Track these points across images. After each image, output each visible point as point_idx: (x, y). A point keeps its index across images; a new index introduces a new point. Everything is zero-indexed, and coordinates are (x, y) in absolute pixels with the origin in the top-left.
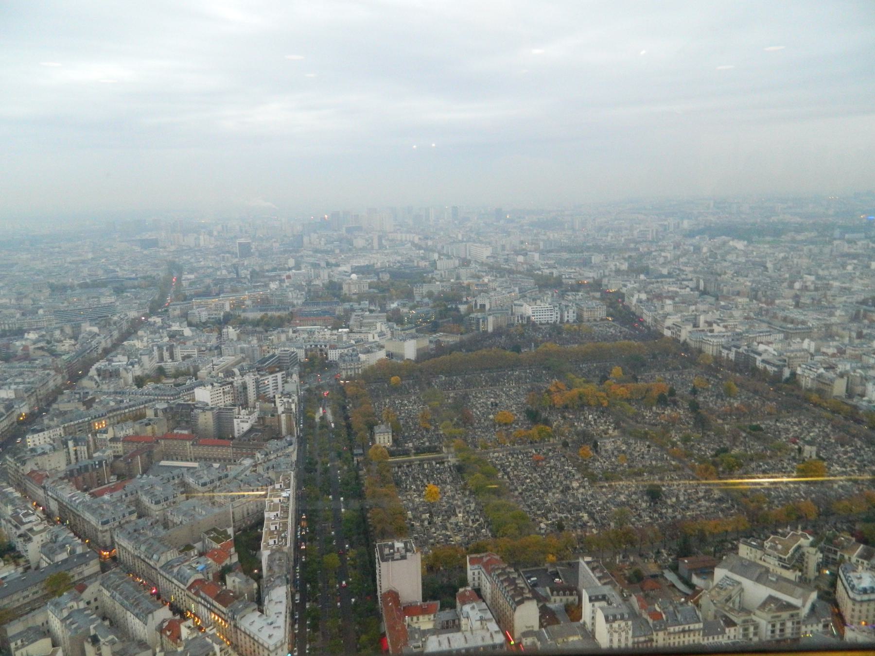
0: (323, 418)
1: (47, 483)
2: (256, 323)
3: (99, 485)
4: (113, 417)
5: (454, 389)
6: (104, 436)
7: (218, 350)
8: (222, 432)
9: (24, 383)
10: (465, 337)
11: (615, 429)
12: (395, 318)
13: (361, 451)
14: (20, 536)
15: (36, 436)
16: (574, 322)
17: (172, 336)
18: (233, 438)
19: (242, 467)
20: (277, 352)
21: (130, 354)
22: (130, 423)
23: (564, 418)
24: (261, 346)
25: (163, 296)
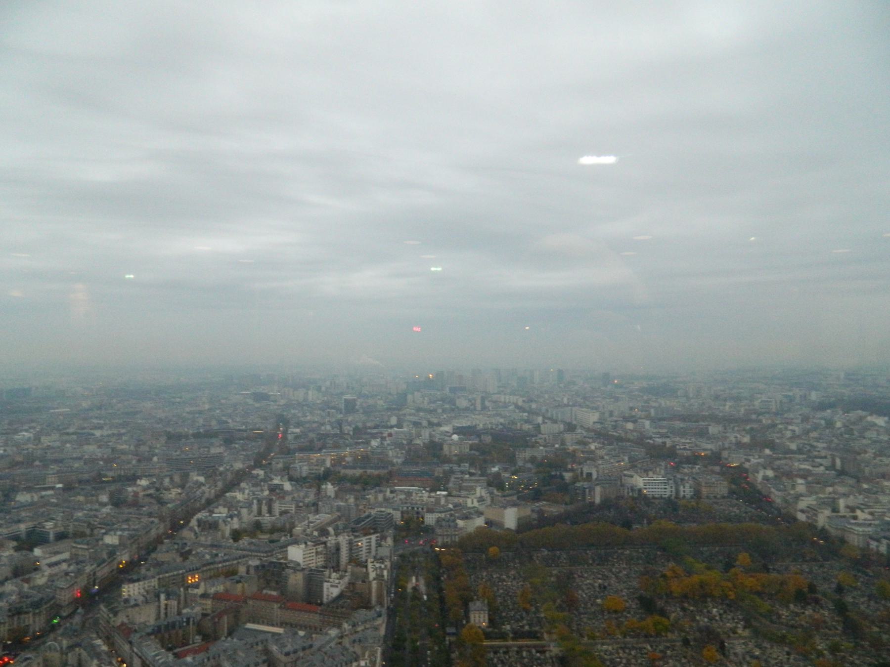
0: (415, 589)
1: (135, 638)
2: (355, 481)
3: (184, 645)
4: (206, 571)
5: (558, 566)
6: (196, 591)
7: (315, 507)
8: (311, 595)
9: (128, 530)
10: (570, 508)
11: (745, 628)
12: (496, 483)
13: (453, 630)
15: (131, 585)
16: (692, 498)
17: (273, 489)
18: (321, 604)
19: (328, 638)
20: (373, 512)
21: (231, 505)
22: (222, 579)
23: (684, 609)
24: (357, 505)
25: (269, 449)
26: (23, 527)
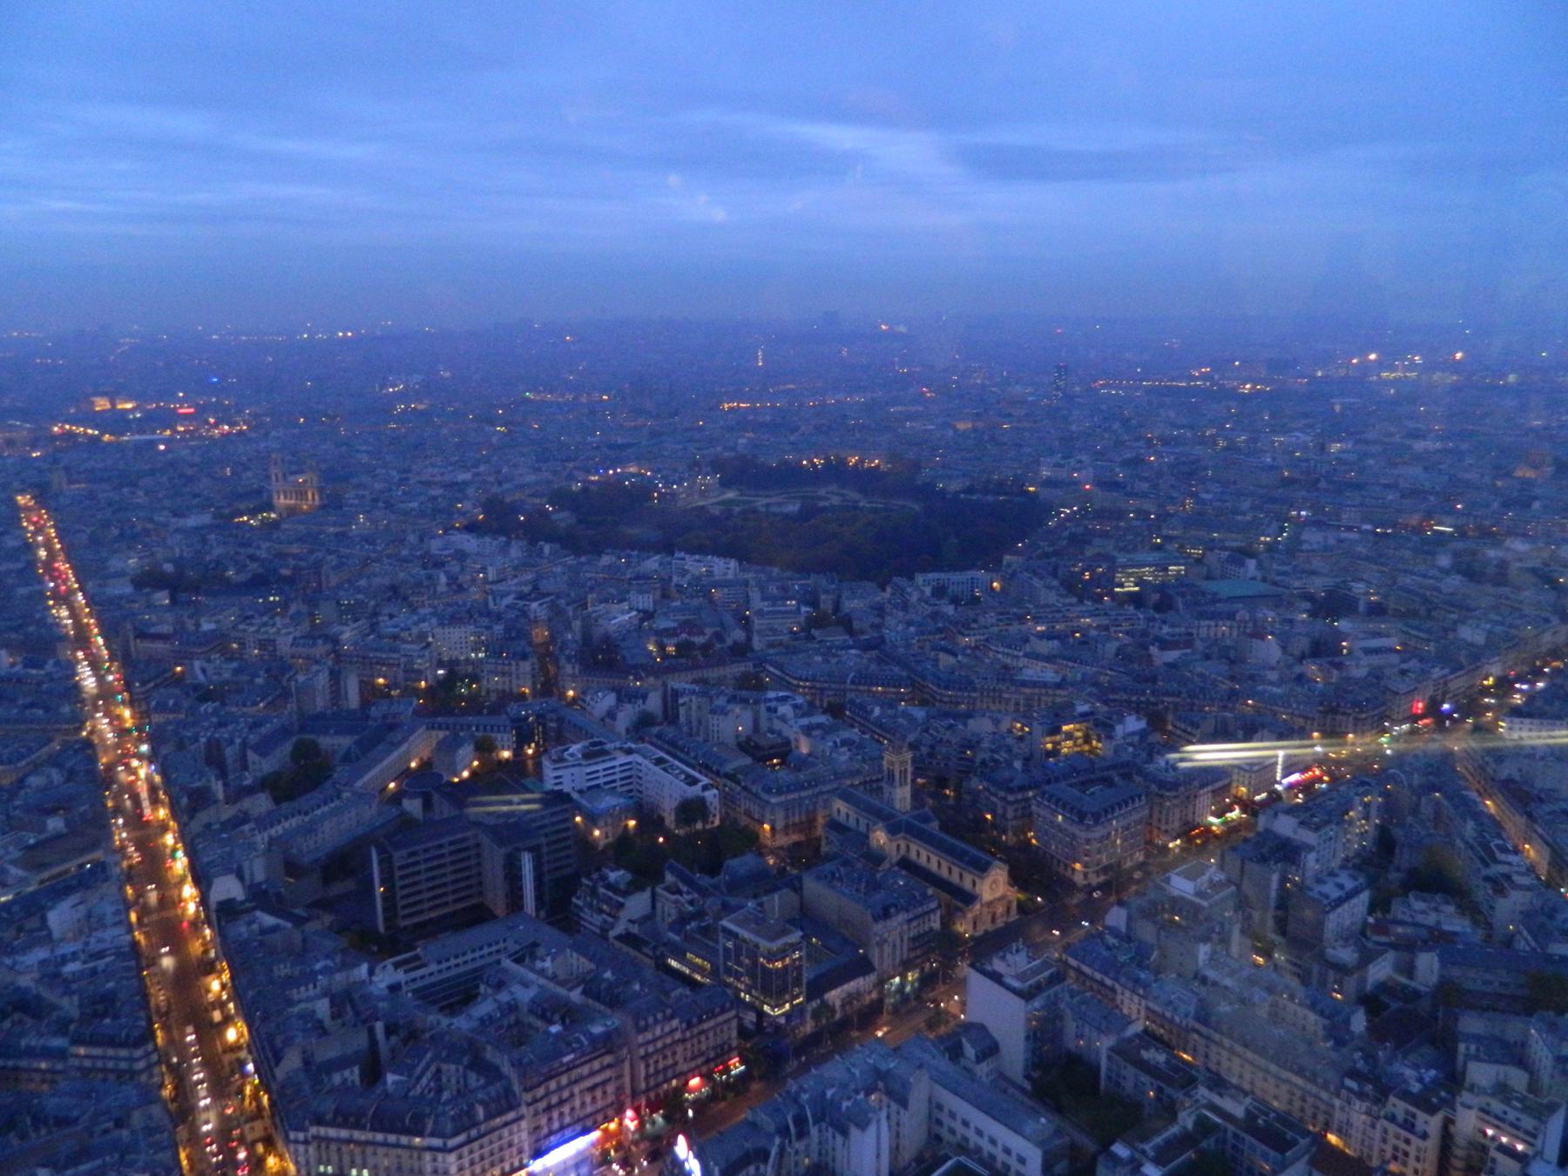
9: (1502, 624)
14: (1487, 879)
26: (1318, 586)
